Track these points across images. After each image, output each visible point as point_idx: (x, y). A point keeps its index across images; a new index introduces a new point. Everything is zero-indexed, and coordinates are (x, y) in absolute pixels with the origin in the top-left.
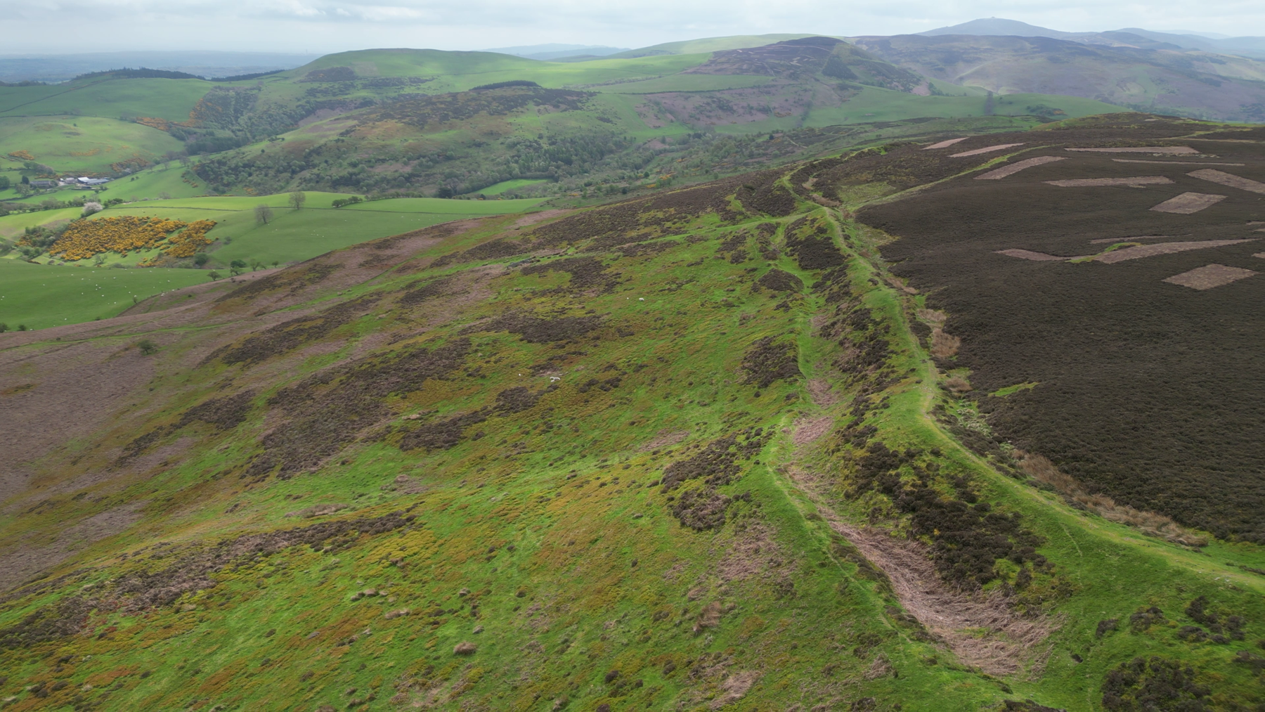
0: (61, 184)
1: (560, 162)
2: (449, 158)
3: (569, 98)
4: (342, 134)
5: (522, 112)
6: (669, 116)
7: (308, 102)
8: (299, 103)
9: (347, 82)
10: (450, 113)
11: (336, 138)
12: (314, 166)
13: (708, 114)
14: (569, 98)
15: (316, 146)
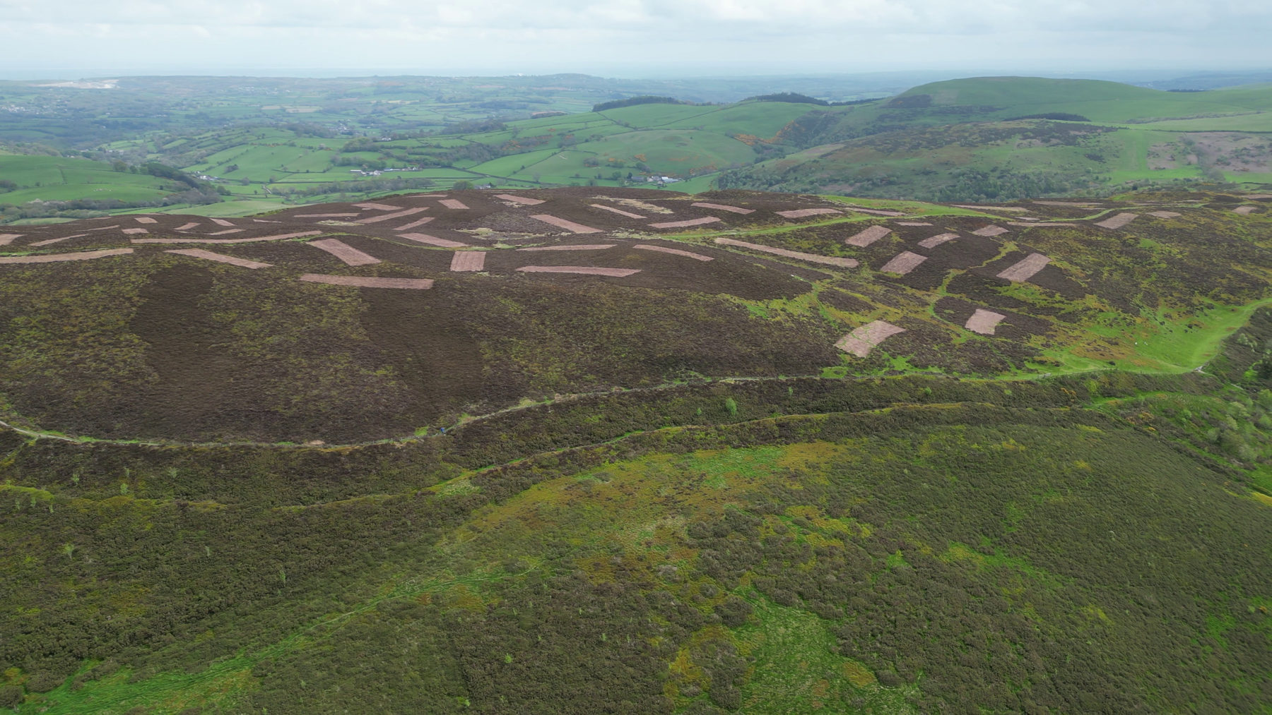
0: (650, 180)
1: (982, 195)
2: (891, 183)
3: (1072, 133)
4: (822, 156)
5: (998, 145)
6: (1193, 158)
7: (874, 126)
8: (867, 127)
9: (919, 109)
10: (924, 143)
11: (812, 160)
12: (786, 181)
13: (1246, 158)
14: (1072, 133)
15: (796, 165)
